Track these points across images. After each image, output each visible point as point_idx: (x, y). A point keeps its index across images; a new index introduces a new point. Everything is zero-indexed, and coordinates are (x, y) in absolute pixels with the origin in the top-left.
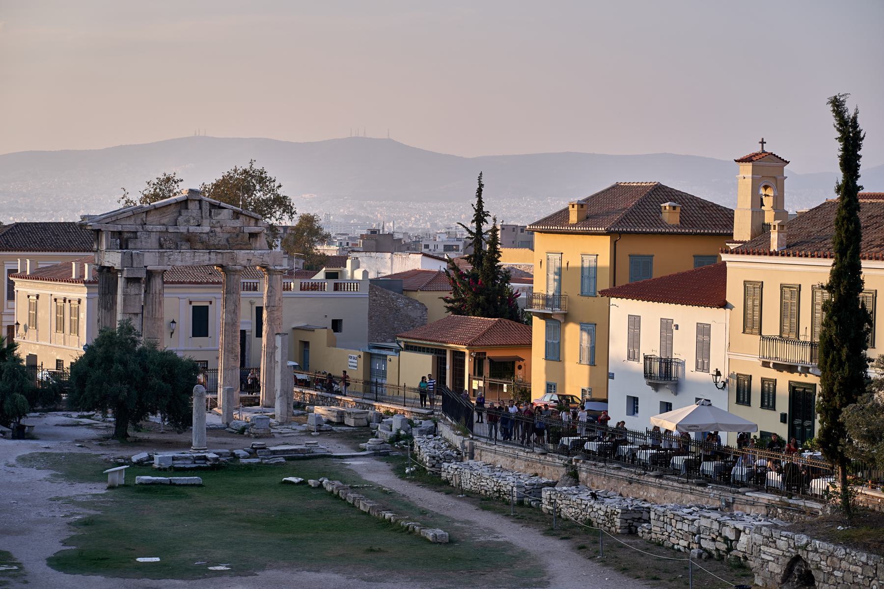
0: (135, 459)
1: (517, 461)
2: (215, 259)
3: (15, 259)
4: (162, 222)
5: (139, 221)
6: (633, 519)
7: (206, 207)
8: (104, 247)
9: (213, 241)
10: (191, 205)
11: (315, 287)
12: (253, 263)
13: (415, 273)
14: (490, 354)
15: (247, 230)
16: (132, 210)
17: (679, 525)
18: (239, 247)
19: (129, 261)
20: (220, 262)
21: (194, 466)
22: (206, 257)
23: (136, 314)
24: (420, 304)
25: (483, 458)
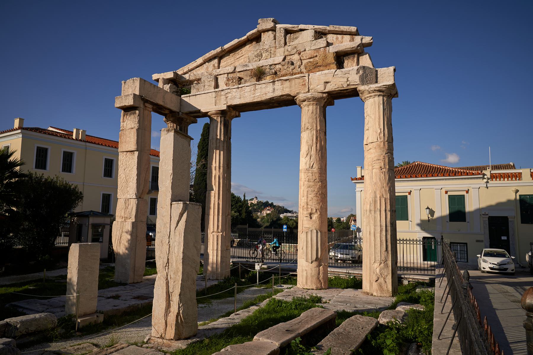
20: (286, 91)
22: (270, 87)
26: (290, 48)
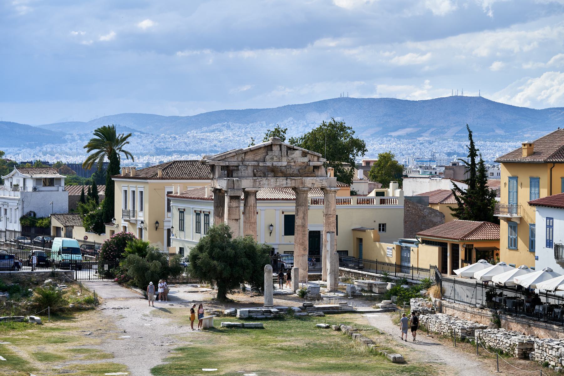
0: (227, 311)
1: (466, 314)
2: (290, 183)
3: (171, 185)
4: (256, 159)
5: (240, 159)
6: (527, 349)
7: (284, 150)
8: (217, 176)
9: (290, 171)
10: (274, 148)
11: (369, 201)
12: (315, 186)
13: (440, 192)
14: (475, 246)
15: (312, 164)
16: (235, 152)
17: (550, 352)
18: (306, 175)
19: (231, 186)
20: (293, 185)
21: (264, 316)
22: (285, 182)
23: (237, 220)
24: (440, 212)
25: (447, 312)
26: (290, 159)
